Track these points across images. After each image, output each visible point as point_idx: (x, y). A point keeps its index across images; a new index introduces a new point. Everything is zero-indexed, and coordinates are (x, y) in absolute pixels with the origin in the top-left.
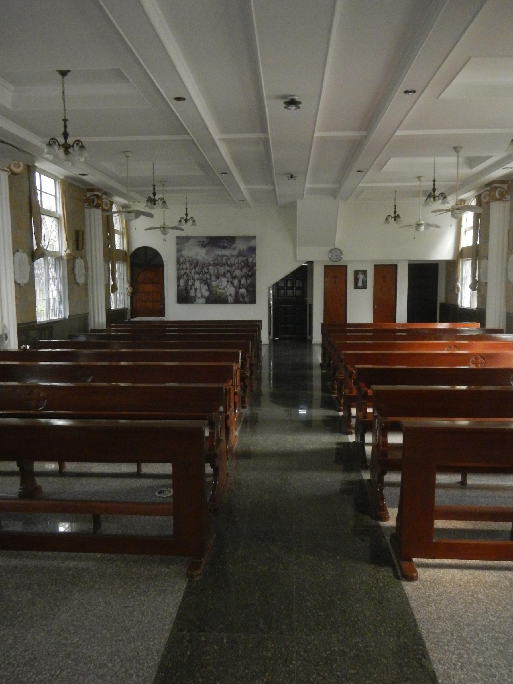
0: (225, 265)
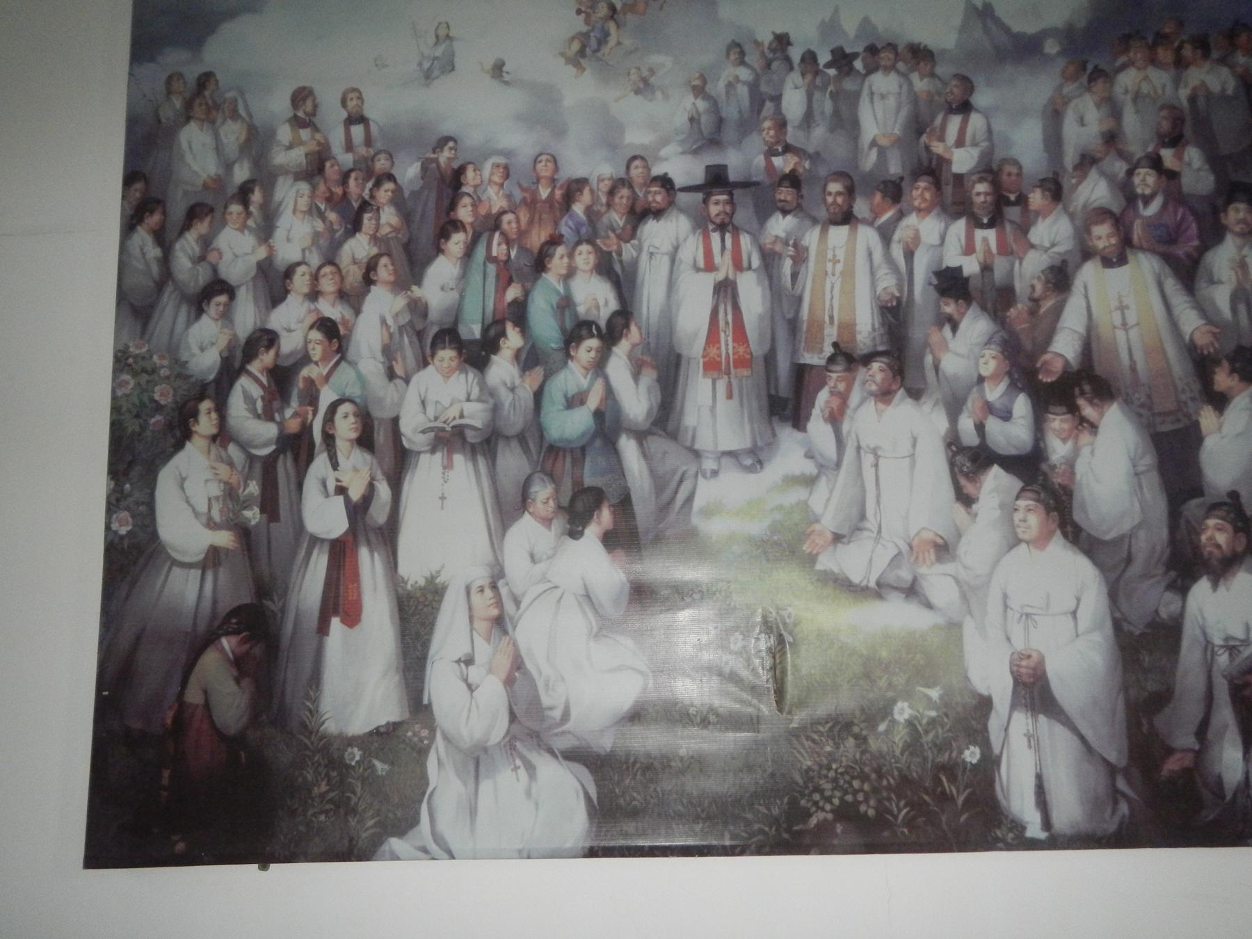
0: (894, 191)
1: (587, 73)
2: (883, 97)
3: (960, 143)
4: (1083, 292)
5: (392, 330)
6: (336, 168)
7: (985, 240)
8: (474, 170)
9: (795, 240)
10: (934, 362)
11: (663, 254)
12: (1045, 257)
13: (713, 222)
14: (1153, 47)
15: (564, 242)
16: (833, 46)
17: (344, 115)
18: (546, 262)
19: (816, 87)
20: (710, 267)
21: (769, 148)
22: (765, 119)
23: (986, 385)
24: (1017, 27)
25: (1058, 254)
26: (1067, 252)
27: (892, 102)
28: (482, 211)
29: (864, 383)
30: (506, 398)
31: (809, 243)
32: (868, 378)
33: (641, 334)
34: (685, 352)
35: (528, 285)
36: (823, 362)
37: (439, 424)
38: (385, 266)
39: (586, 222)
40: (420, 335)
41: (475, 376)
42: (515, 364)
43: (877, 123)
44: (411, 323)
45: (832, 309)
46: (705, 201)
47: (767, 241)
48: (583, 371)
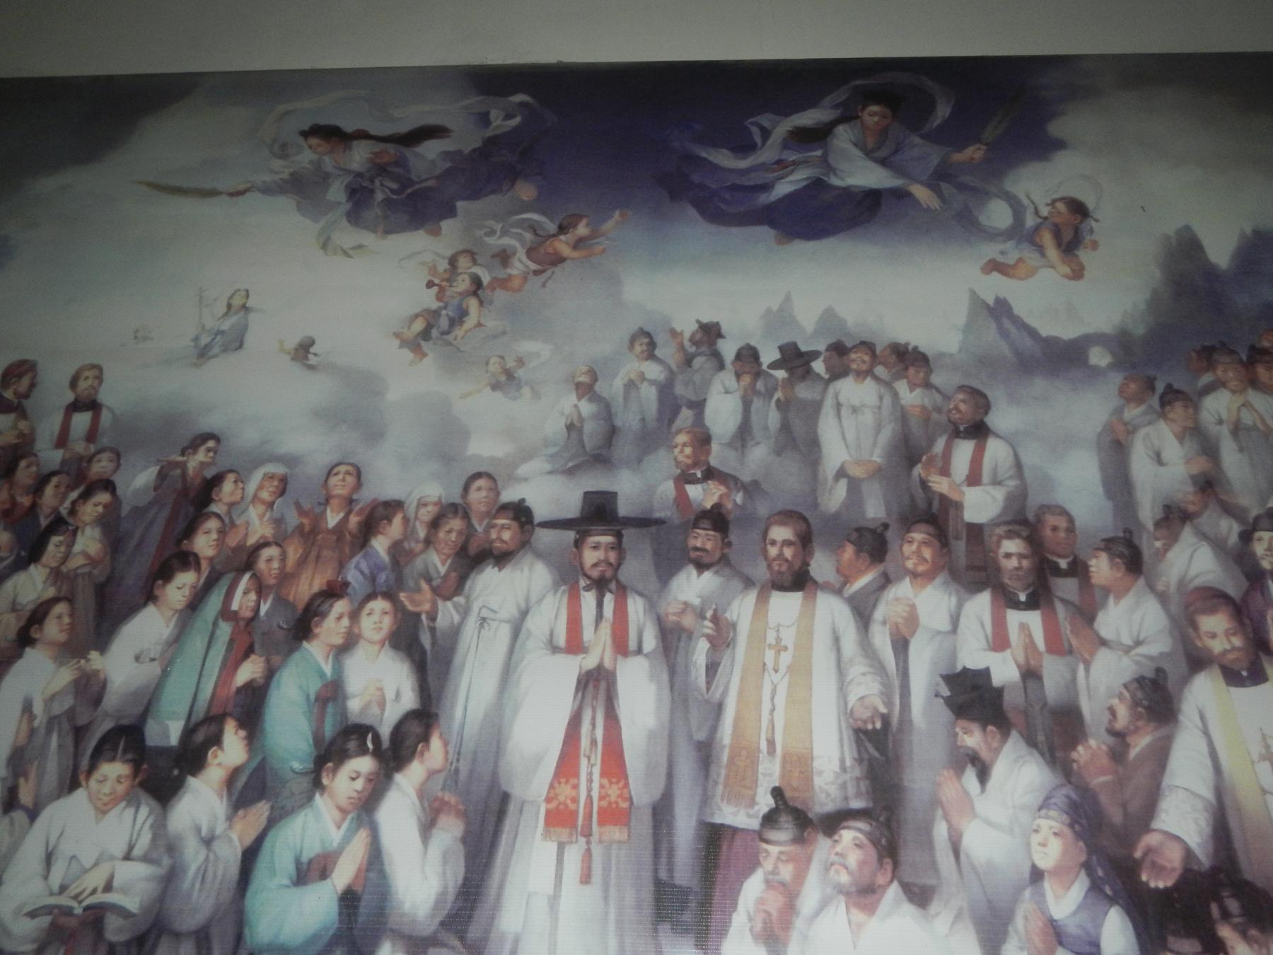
1: (428, 361)
2: (855, 410)
3: (974, 479)
4: (1199, 723)
5: (36, 723)
6: (34, 469)
7: (1024, 627)
8: (236, 482)
9: (715, 610)
10: (949, 833)
11: (502, 621)
12: (1126, 661)
13: (585, 575)
14: (1250, 364)
15: (347, 594)
16: (785, 340)
17: (70, 397)
18: (313, 624)
19: (756, 393)
20: (575, 645)
21: (683, 471)
22: (679, 432)
23: (1047, 885)
24: (1047, 329)
25: (1151, 658)
26: (1162, 655)
27: (868, 418)
28: (232, 541)
29: (828, 867)
30: (193, 855)
31: (738, 616)
32: (833, 858)
33: (447, 753)
34: (516, 791)
35: (276, 659)
36: (755, 824)
37: (64, 901)
38: (59, 617)
39: (389, 566)
40: (79, 733)
41: (150, 813)
42: (225, 793)
43: (847, 446)
44: (71, 714)
45: (773, 726)
46: (578, 544)
47: (671, 609)
48: (337, 815)
